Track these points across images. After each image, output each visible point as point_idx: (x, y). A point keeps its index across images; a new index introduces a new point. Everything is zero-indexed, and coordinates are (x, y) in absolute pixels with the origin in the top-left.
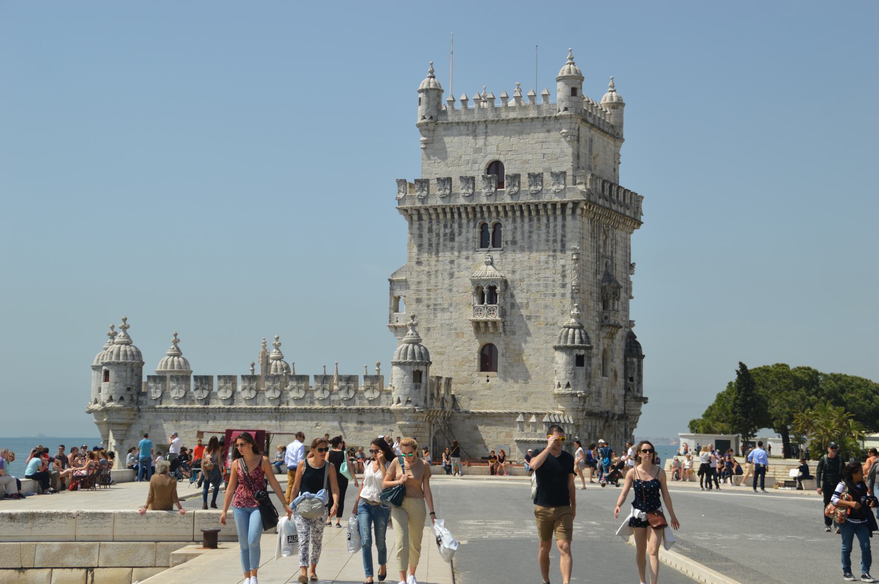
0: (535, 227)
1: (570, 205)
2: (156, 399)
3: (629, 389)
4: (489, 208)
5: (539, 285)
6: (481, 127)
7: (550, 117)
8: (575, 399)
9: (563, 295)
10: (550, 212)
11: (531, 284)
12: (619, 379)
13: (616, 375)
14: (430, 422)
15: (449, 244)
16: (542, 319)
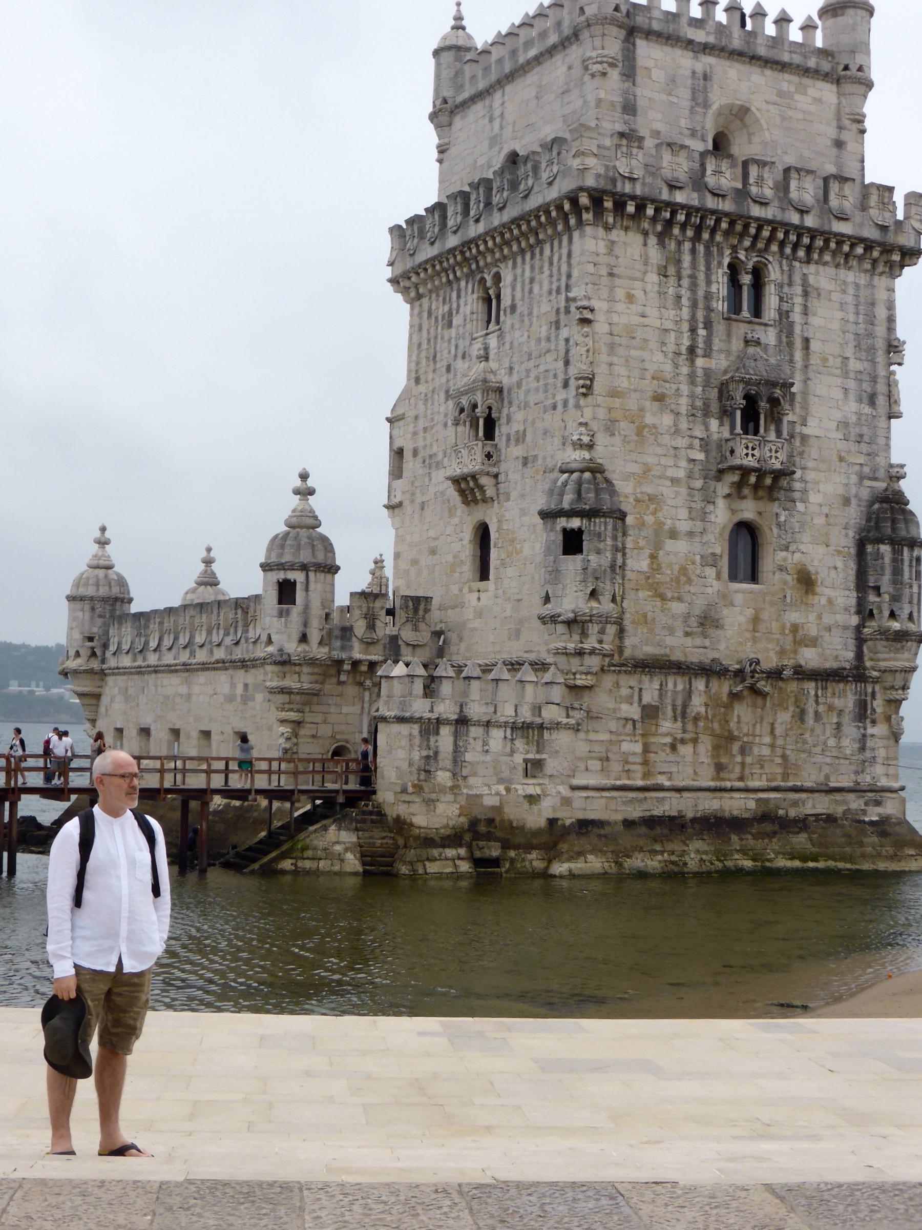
0: (537, 270)
1: (567, 207)
2: (114, 654)
3: (871, 614)
4: (477, 246)
5: (537, 390)
6: (498, 95)
7: (568, 38)
8: (561, 628)
9: (565, 403)
10: (550, 231)
11: (529, 391)
12: (818, 590)
13: (806, 581)
14: (361, 684)
15: (446, 333)
16: (540, 462)
